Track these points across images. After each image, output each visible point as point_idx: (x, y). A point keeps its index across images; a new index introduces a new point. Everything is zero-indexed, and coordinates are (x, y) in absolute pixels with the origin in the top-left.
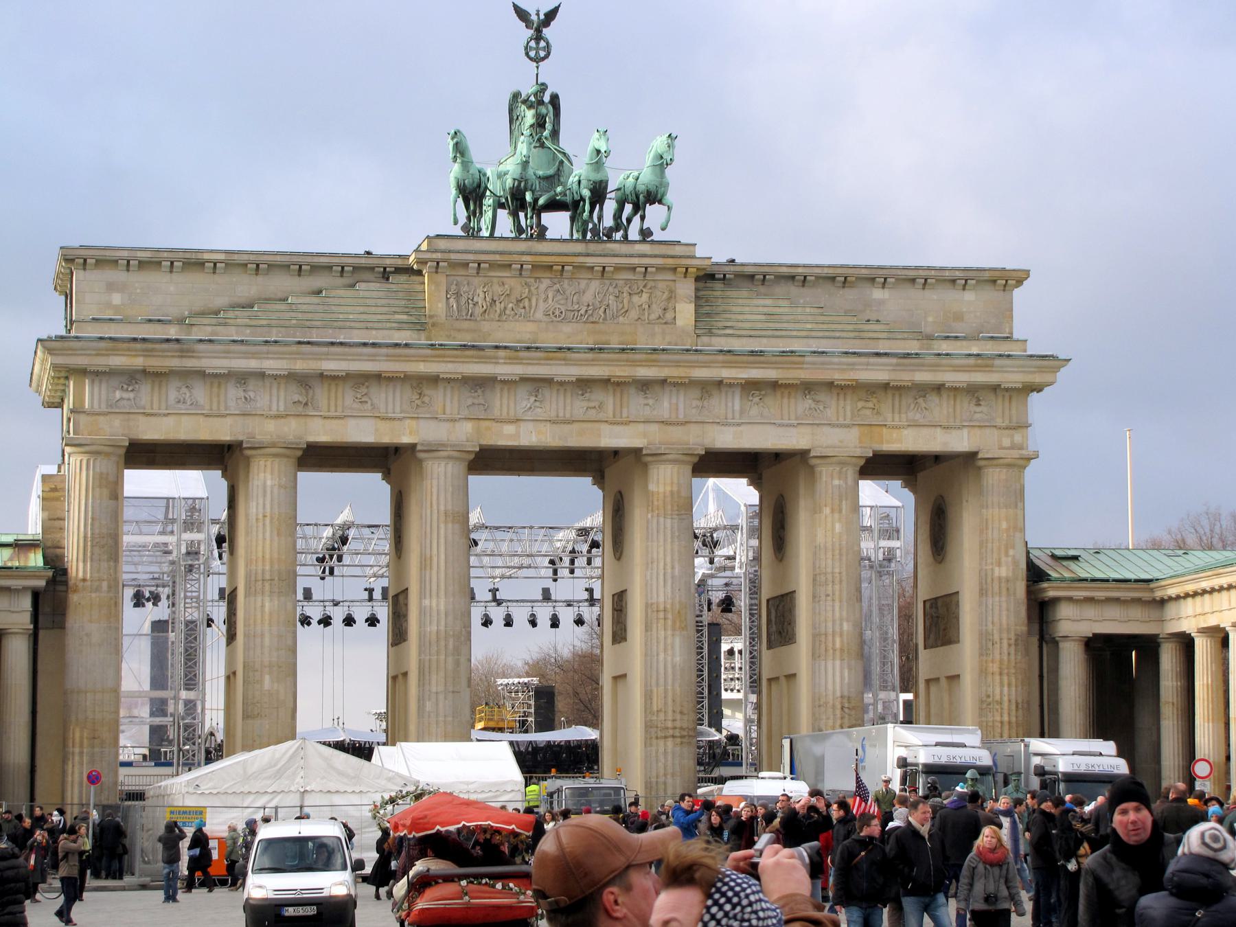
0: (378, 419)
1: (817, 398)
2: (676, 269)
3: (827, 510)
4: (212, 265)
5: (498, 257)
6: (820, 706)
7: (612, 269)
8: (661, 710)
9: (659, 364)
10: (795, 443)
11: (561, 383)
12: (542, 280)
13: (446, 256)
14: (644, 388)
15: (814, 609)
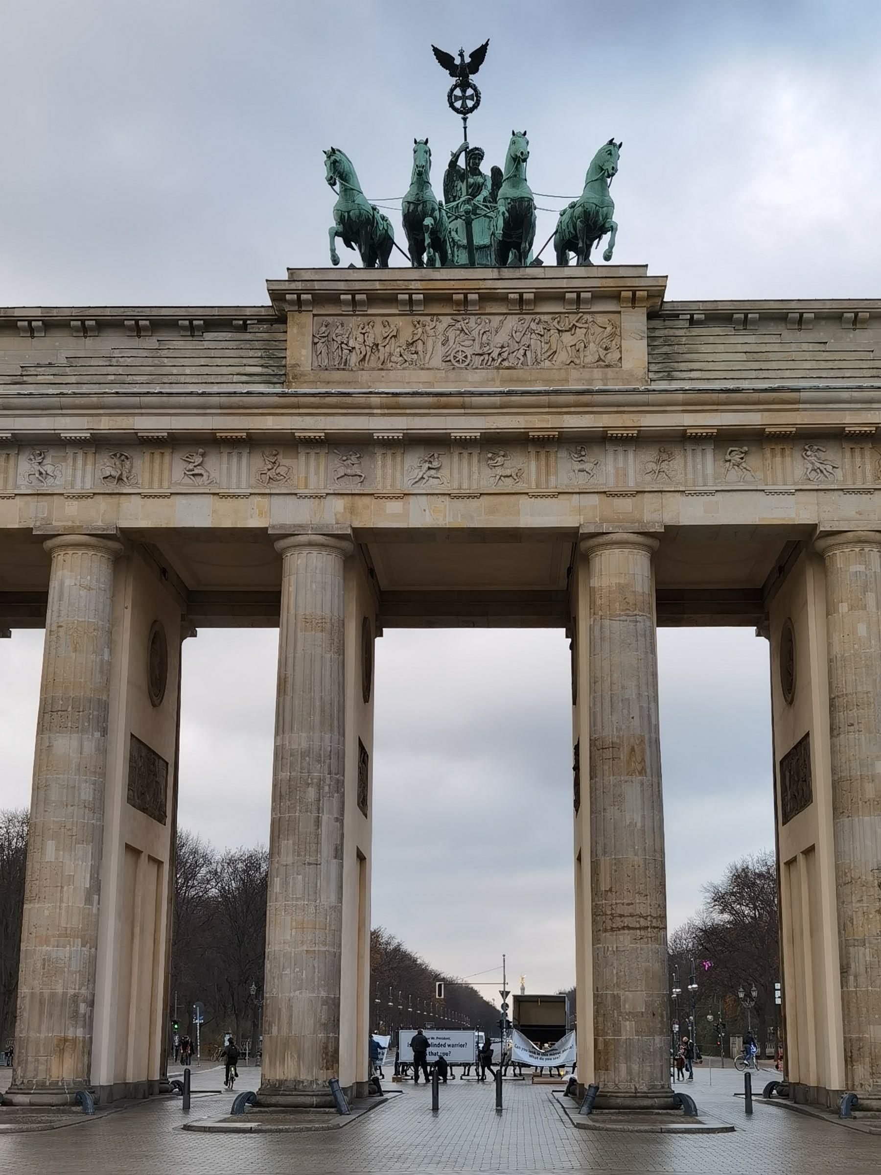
0: (216, 497)
1: (821, 455)
2: (615, 296)
3: (843, 608)
4: (26, 323)
5: (377, 285)
6: (845, 884)
7: (532, 296)
8: (610, 890)
9: (595, 409)
10: (793, 515)
11: (465, 444)
12: (441, 317)
13: (309, 285)
14: (579, 448)
15: (833, 746)
